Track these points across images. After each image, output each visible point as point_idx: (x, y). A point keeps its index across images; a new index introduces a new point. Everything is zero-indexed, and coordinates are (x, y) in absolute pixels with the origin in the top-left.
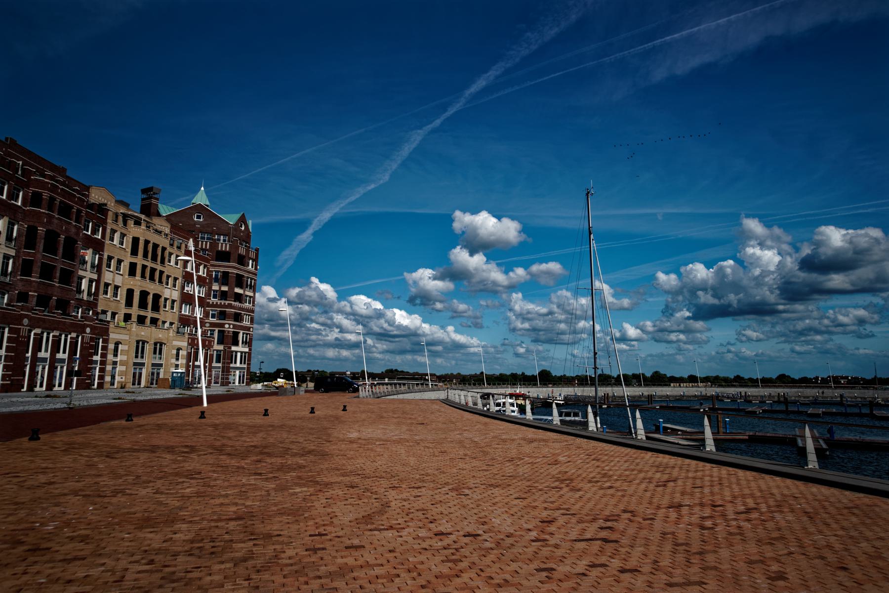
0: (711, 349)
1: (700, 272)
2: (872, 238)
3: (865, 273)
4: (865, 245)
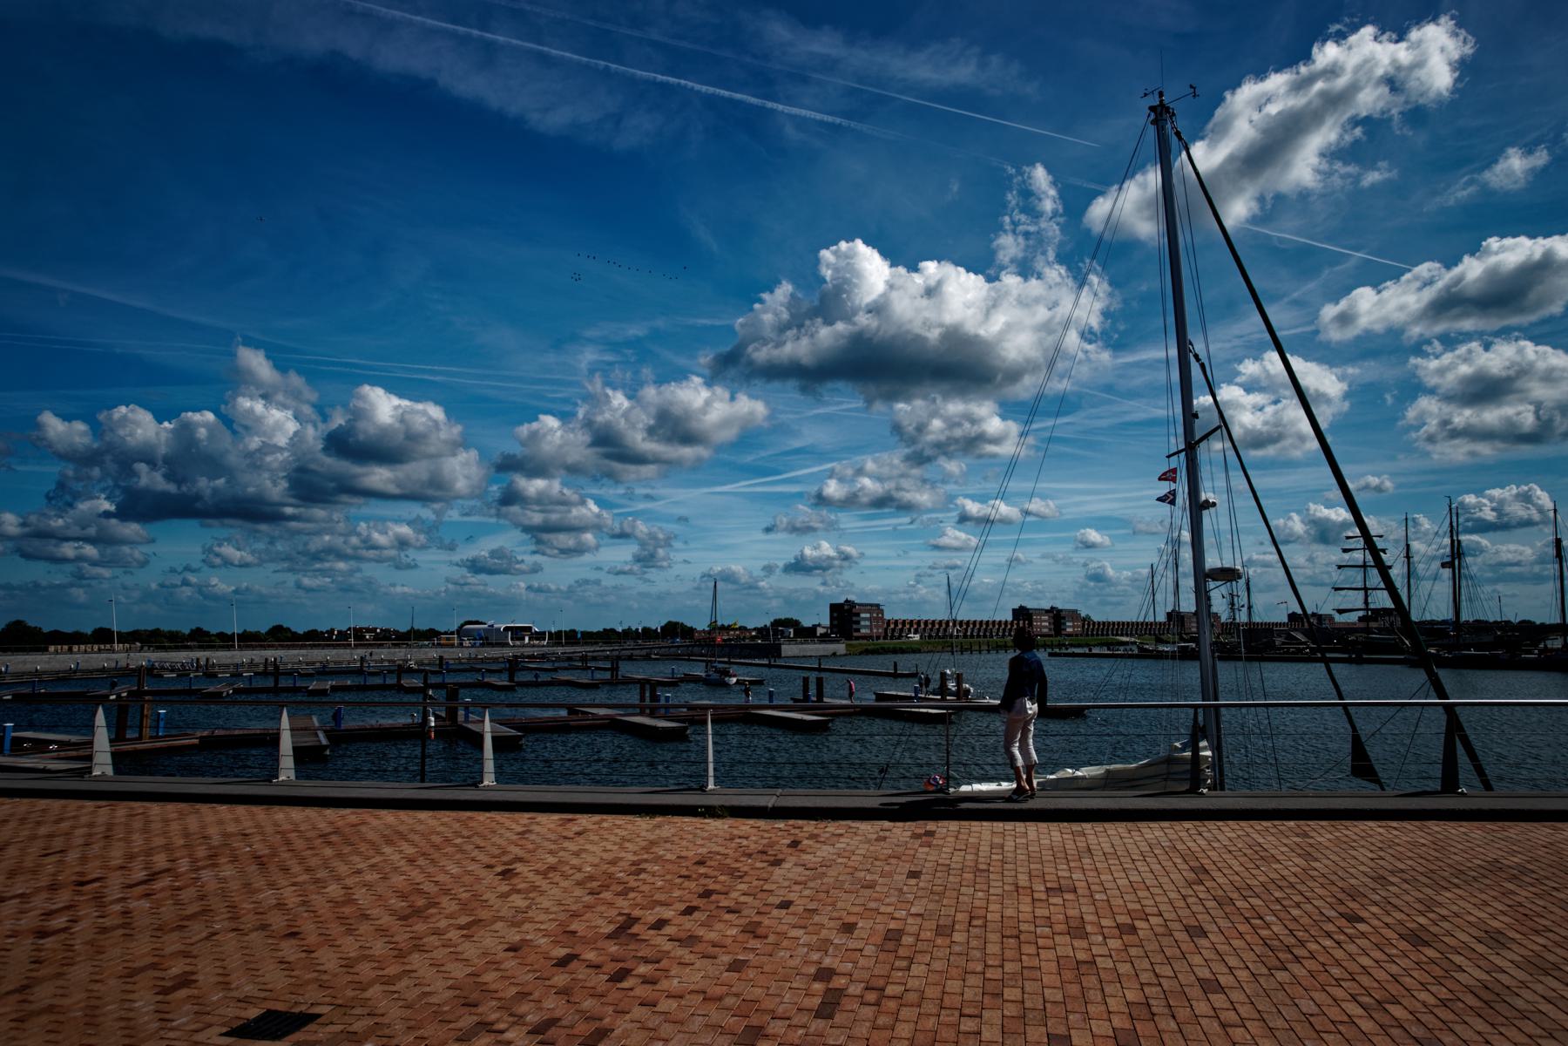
0: (150, 579)
1: (142, 426)
2: (430, 418)
3: (416, 471)
4: (422, 429)
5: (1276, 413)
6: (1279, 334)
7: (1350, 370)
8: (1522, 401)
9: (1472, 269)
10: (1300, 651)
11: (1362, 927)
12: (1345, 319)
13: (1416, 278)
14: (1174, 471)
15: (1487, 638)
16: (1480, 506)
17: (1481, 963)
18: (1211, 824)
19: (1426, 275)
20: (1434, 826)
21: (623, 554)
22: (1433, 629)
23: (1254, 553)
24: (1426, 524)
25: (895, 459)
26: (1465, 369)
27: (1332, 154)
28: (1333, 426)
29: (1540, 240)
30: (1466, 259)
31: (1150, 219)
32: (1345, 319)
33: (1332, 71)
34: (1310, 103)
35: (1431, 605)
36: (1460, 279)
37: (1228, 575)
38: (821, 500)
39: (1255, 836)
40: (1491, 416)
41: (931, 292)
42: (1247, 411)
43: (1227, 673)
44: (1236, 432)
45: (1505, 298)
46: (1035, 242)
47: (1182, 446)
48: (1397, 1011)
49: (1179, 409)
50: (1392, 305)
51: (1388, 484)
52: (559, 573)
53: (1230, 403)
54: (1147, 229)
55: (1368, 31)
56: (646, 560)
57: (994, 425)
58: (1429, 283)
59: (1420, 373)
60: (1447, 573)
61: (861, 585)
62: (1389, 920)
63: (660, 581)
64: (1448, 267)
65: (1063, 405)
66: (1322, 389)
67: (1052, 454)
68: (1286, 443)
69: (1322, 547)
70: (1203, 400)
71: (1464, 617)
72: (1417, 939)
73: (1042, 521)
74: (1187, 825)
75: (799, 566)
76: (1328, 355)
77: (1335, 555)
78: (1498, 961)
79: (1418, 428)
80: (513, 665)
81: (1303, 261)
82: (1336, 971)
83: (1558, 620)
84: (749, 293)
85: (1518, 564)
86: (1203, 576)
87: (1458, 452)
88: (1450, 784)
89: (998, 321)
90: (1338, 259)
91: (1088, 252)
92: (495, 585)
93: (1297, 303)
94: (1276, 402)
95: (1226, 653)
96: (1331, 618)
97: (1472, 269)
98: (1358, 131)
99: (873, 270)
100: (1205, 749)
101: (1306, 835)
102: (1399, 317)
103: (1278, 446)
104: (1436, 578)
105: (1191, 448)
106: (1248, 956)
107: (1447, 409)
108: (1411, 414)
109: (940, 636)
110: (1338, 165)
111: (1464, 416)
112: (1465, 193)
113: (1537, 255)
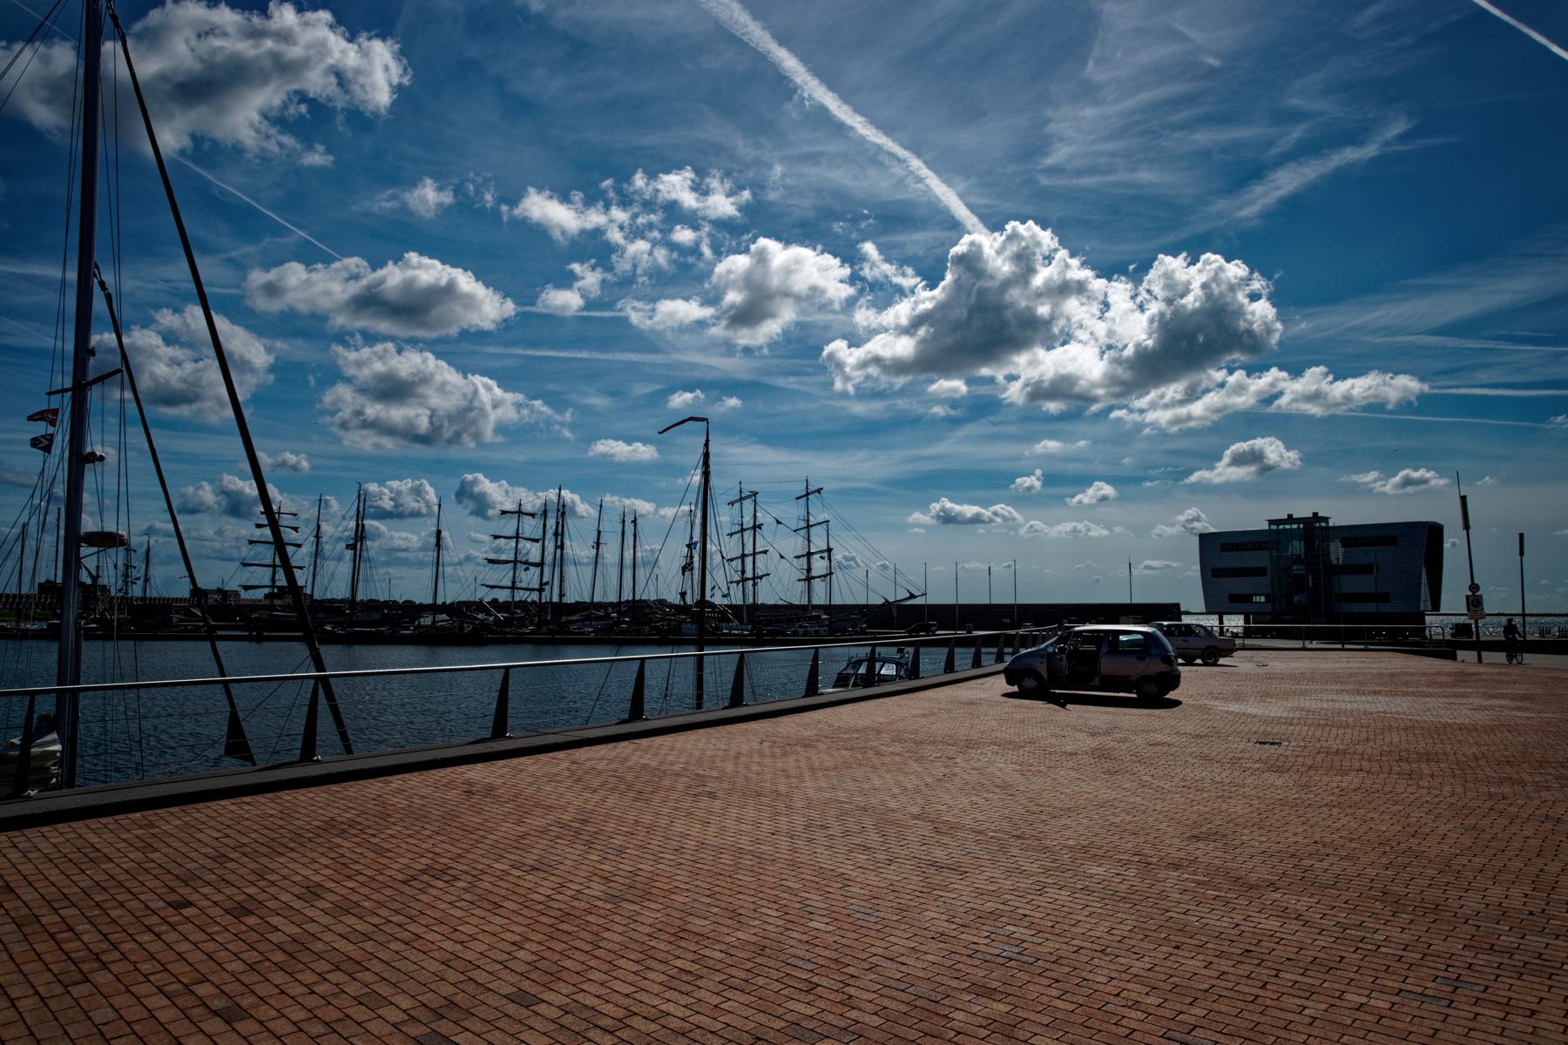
5: (197, 371)
6: (206, 289)
7: (279, 344)
8: (422, 405)
9: (392, 276)
10: (198, 628)
11: (187, 912)
12: (272, 290)
13: (345, 268)
14: (55, 412)
15: (377, 616)
16: (380, 495)
17: (295, 919)
18: (32, 833)
19: (354, 270)
20: (286, 795)
22: (331, 608)
23: (143, 520)
24: (335, 505)
26: (379, 367)
27: (278, 120)
28: (258, 398)
29: (448, 269)
30: (390, 263)
31: (48, 102)
32: (272, 290)
33: (285, 36)
34: (258, 57)
35: (333, 584)
36: (382, 281)
40: (397, 414)
42: (161, 360)
43: (92, 653)
44: (144, 383)
45: (414, 308)
47: (68, 383)
48: (203, 990)
49: (70, 346)
50: (318, 289)
51: (305, 464)
53: (138, 350)
55: (325, 16)
58: (355, 277)
59: (341, 362)
60: (350, 553)
62: (218, 897)
64: (374, 269)
66: (247, 357)
68: (207, 405)
69: (233, 520)
70: (103, 338)
71: (359, 597)
72: (241, 910)
77: (246, 529)
78: (310, 912)
79: (333, 413)
82: (146, 967)
83: (429, 600)
85: (406, 550)
86: (74, 538)
88: (308, 753)
90: (280, 231)
93: (232, 262)
94: (196, 361)
95: (105, 632)
96: (236, 594)
97: (392, 276)
98: (303, 108)
100: (53, 742)
101: (152, 826)
102: (324, 303)
103: (195, 407)
104: (340, 558)
105: (80, 389)
106: (41, 980)
107: (361, 400)
108: (328, 398)
110: (273, 131)
111: (373, 410)
112: (388, 205)
113: (444, 282)
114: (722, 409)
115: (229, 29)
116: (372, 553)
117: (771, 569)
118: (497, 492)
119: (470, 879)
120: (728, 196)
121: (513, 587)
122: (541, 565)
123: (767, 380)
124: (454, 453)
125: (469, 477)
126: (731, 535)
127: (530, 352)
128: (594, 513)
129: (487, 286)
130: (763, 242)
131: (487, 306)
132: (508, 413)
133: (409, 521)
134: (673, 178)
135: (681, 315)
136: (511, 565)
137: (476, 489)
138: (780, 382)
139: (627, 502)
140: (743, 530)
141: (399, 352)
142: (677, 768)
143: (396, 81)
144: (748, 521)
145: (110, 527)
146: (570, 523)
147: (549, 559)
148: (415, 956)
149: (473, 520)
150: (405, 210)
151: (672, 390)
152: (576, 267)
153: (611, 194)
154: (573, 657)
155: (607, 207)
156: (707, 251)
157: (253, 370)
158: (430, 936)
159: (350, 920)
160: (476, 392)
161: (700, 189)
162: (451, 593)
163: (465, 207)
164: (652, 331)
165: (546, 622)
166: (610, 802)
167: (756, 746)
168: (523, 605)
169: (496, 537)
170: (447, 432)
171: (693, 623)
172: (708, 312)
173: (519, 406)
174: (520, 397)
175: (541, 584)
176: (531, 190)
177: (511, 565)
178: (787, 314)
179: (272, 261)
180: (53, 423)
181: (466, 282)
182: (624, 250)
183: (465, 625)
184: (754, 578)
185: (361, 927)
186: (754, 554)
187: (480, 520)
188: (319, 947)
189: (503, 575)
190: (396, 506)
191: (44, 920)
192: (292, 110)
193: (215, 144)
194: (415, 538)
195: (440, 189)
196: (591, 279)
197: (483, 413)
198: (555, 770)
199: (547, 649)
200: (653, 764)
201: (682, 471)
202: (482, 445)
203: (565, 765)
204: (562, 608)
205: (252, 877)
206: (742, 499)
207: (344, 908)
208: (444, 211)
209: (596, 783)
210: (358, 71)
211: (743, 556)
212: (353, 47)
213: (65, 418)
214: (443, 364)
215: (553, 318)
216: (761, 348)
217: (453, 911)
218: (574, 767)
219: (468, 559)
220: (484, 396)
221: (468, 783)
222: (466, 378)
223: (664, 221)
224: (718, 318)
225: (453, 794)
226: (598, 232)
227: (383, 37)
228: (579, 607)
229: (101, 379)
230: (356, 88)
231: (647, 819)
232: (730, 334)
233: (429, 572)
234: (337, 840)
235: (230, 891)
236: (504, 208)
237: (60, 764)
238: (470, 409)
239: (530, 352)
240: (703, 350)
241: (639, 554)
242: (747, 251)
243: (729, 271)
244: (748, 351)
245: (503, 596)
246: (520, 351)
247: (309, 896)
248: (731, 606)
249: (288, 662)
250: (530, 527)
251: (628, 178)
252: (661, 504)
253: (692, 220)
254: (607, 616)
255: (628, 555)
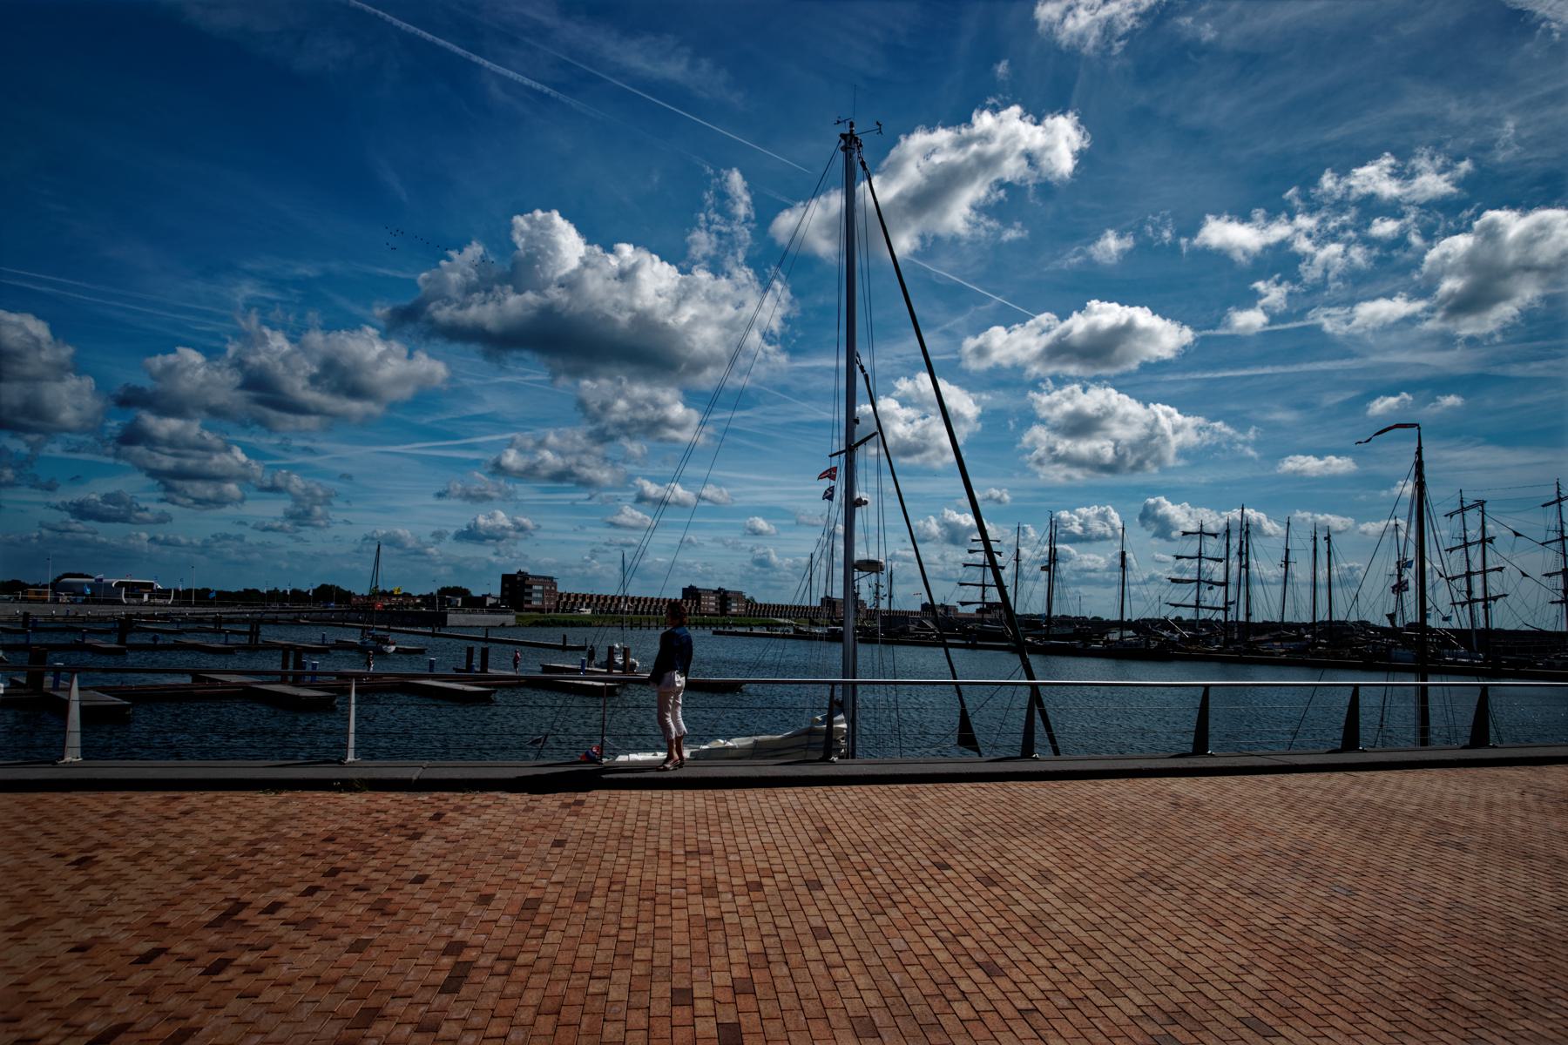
2: (28, 334)
4: (15, 345)
5: (924, 426)
6: (932, 358)
7: (984, 397)
8: (1106, 437)
9: (1078, 324)
11: (949, 873)
12: (981, 352)
13: (1038, 325)
14: (835, 469)
15: (1070, 631)
16: (1071, 521)
17: (1034, 897)
18: (837, 789)
19: (1045, 324)
20: (1013, 786)
21: (273, 509)
22: (1031, 622)
24: (1032, 533)
25: (578, 435)
26: (1068, 407)
27: (981, 209)
28: (967, 443)
29: (1126, 308)
30: (1075, 314)
31: (829, 238)
33: (986, 138)
34: (966, 161)
35: (1032, 603)
36: (1069, 331)
37: (872, 566)
38: (498, 469)
39: (874, 798)
40: (1084, 447)
41: (626, 275)
42: (900, 422)
43: (865, 652)
44: (890, 440)
45: (1099, 351)
46: (727, 242)
48: (967, 942)
49: (843, 416)
50: (1018, 345)
51: (1007, 497)
52: (190, 525)
53: (886, 414)
54: (826, 247)
55: (1016, 110)
56: (300, 518)
57: (678, 411)
58: (1046, 330)
59: (1036, 406)
60: (1044, 574)
61: (534, 558)
63: (314, 541)
64: (1062, 320)
65: (742, 399)
66: (961, 410)
67: (726, 443)
68: (930, 454)
69: (952, 547)
70: (864, 408)
71: (1054, 613)
72: (989, 881)
73: (716, 508)
74: (817, 789)
75: (471, 535)
76: (969, 382)
77: (960, 555)
78: (1045, 894)
79: (1031, 452)
80: (126, 626)
81: (955, 297)
82: (924, 913)
83: (1118, 618)
84: (437, 248)
85: (1094, 571)
86: (851, 566)
87: (1057, 475)
88: (1027, 751)
89: (688, 312)
90: (983, 300)
91: (777, 261)
92: (108, 534)
93: (947, 333)
94: (924, 418)
95: (868, 637)
96: (955, 609)
97: (1078, 324)
98: (1002, 193)
99: (570, 245)
100: (840, 722)
102: (1022, 356)
103: (923, 456)
104: (1037, 579)
105: (850, 449)
106: (856, 904)
107: (1053, 438)
108: (1026, 439)
109: (611, 611)
110: (983, 219)
111: (1064, 445)
113: (1123, 322)
114: (1435, 410)
115: (946, 145)
116: (1064, 574)
117: (1510, 589)
118: (1179, 514)
119: (1187, 891)
120: (1440, 172)
121: (1197, 606)
122: (1225, 584)
123: (1498, 370)
124: (1137, 479)
125: (1152, 501)
126: (1451, 550)
127: (1208, 375)
128: (1282, 530)
129: (1164, 318)
130: (1490, 215)
131: (1165, 336)
132: (1190, 437)
133: (1097, 544)
134: (1369, 170)
135: (1384, 314)
136: (1194, 585)
137: (1159, 512)
138: (1516, 370)
139: (1320, 518)
140: (1466, 545)
141: (1085, 390)
142: (1410, 809)
143: (1077, 148)
144: (1474, 533)
145: (873, 557)
146: (1255, 542)
147: (1233, 578)
148: (1141, 954)
149: (1156, 542)
150: (1090, 262)
151: (1373, 395)
152: (1260, 285)
153: (1297, 202)
154: (1264, 678)
155: (1291, 218)
156: (1416, 240)
157: (966, 421)
158: (1155, 939)
159: (1078, 907)
160: (1156, 420)
161: (1402, 174)
162: (1135, 612)
163: (1145, 248)
164: (1349, 336)
165: (1232, 641)
166: (1331, 835)
167: (1515, 797)
168: (1207, 623)
169: (1178, 557)
170: (1131, 460)
171: (1408, 648)
172: (1418, 306)
173: (1199, 429)
174: (1200, 420)
175: (1226, 603)
176: (1209, 218)
177: (1194, 585)
178: (1528, 292)
179: (980, 328)
180: (833, 478)
181: (1143, 317)
182: (1312, 257)
183: (1149, 642)
184: (1485, 599)
185: (1090, 917)
186: (1484, 572)
187: (1163, 541)
188: (1055, 926)
189: (1187, 594)
190: (1085, 530)
191: (853, 859)
192: (993, 197)
193: (937, 238)
194: (1102, 560)
195: (1121, 236)
196: (1274, 294)
197: (1166, 441)
198: (1263, 794)
199: (1233, 668)
200: (1378, 800)
201: (1389, 483)
202: (1164, 470)
203: (1274, 789)
204: (1249, 628)
205: (993, 853)
206: (1463, 509)
207: (1072, 896)
208: (1126, 255)
209: (1312, 813)
210: (1045, 149)
211: (1469, 575)
212: (1040, 128)
213: (841, 474)
214: (1125, 397)
215: (1238, 340)
216: (1491, 336)
217: (1174, 920)
218: (1284, 793)
219: (1152, 578)
220: (1165, 423)
221: (1173, 795)
222: (1146, 406)
223: (1358, 219)
224: (1431, 310)
225: (1159, 804)
226: (1283, 244)
227: (1064, 113)
228: (1267, 627)
229: (863, 441)
230: (1044, 163)
231: (1379, 861)
232: (1450, 325)
233: (1115, 591)
234: (1061, 833)
235: (978, 862)
236: (1183, 241)
237: (846, 738)
238: (1151, 437)
239: (1208, 375)
240: (1413, 346)
241: (1334, 572)
242: (1466, 229)
243: (1445, 256)
244: (1472, 341)
245: (1187, 614)
246: (1198, 376)
247: (1041, 879)
248: (1453, 631)
249: (992, 670)
250: (1213, 547)
251: (1314, 180)
252: (1360, 519)
253: (1393, 209)
254: (1300, 637)
255: (1322, 574)
